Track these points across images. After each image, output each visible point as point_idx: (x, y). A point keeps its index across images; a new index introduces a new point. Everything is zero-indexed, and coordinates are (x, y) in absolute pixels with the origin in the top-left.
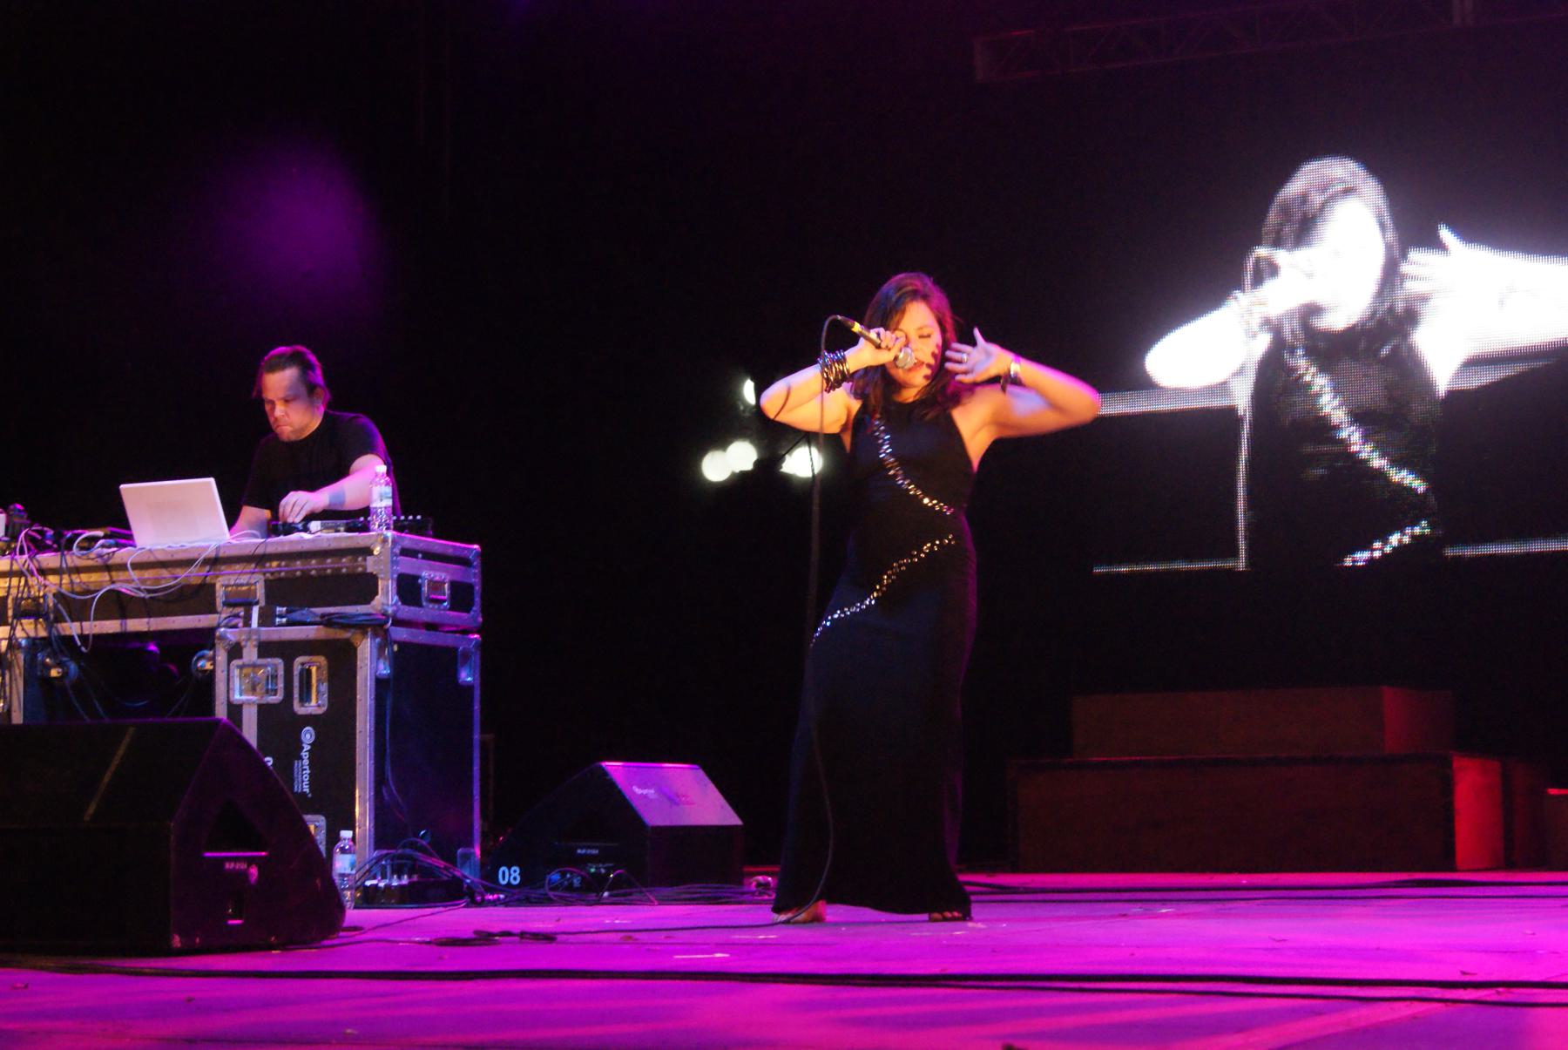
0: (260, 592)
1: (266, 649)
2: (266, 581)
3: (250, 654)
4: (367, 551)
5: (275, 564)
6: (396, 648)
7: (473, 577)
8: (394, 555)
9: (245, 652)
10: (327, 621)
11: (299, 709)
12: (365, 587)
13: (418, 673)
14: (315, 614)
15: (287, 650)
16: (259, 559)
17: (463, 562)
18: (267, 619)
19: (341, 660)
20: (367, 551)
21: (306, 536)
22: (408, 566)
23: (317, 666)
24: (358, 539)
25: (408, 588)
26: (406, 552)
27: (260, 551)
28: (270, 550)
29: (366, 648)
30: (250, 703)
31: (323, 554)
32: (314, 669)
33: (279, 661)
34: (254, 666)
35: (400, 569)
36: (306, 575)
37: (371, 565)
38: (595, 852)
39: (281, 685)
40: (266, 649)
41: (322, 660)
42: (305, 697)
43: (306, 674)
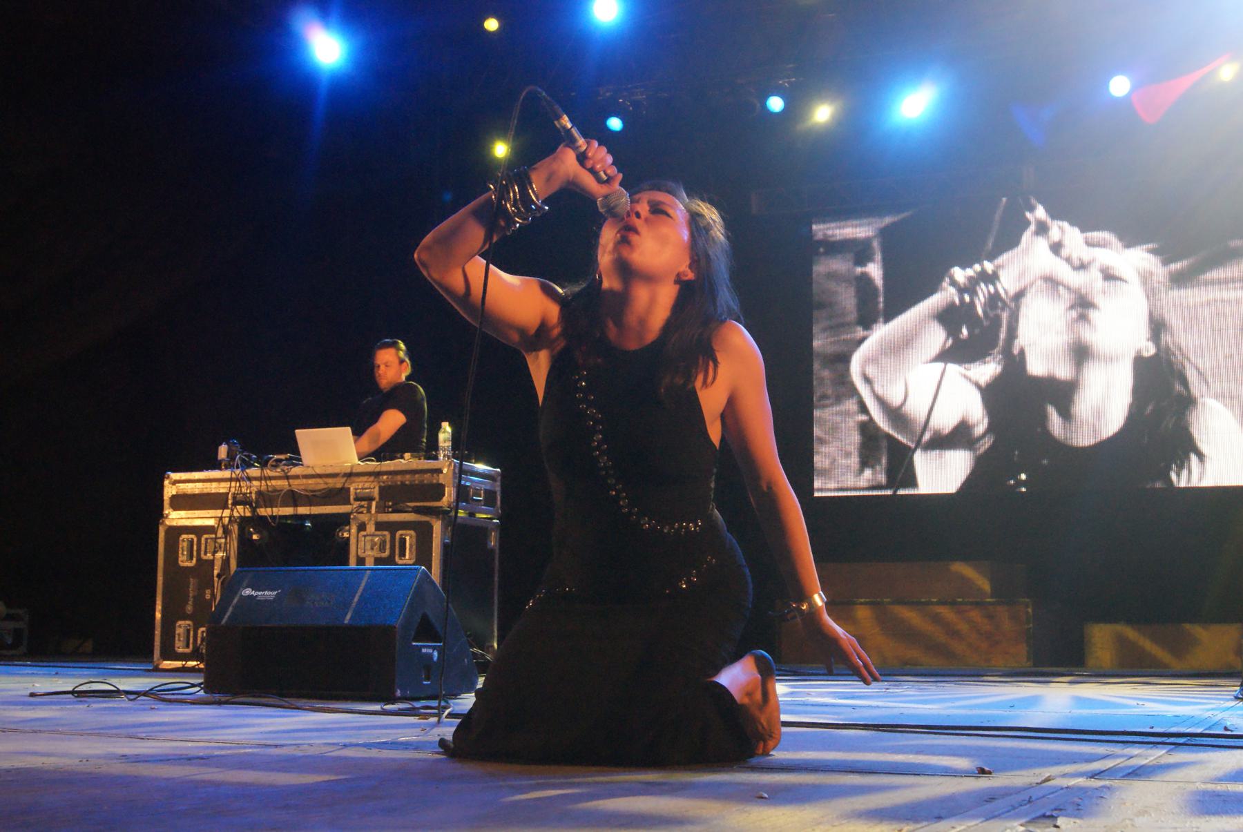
1: (380, 526)
3: (371, 528)
4: (439, 471)
10: (417, 510)
12: (438, 491)
15: (392, 527)
16: (377, 474)
19: (424, 533)
20: (439, 471)
23: (410, 538)
24: (430, 464)
27: (378, 470)
28: (384, 469)
29: (437, 526)
34: (373, 535)
37: (441, 479)
39: (388, 546)
40: (380, 526)
41: (412, 533)
43: (403, 542)
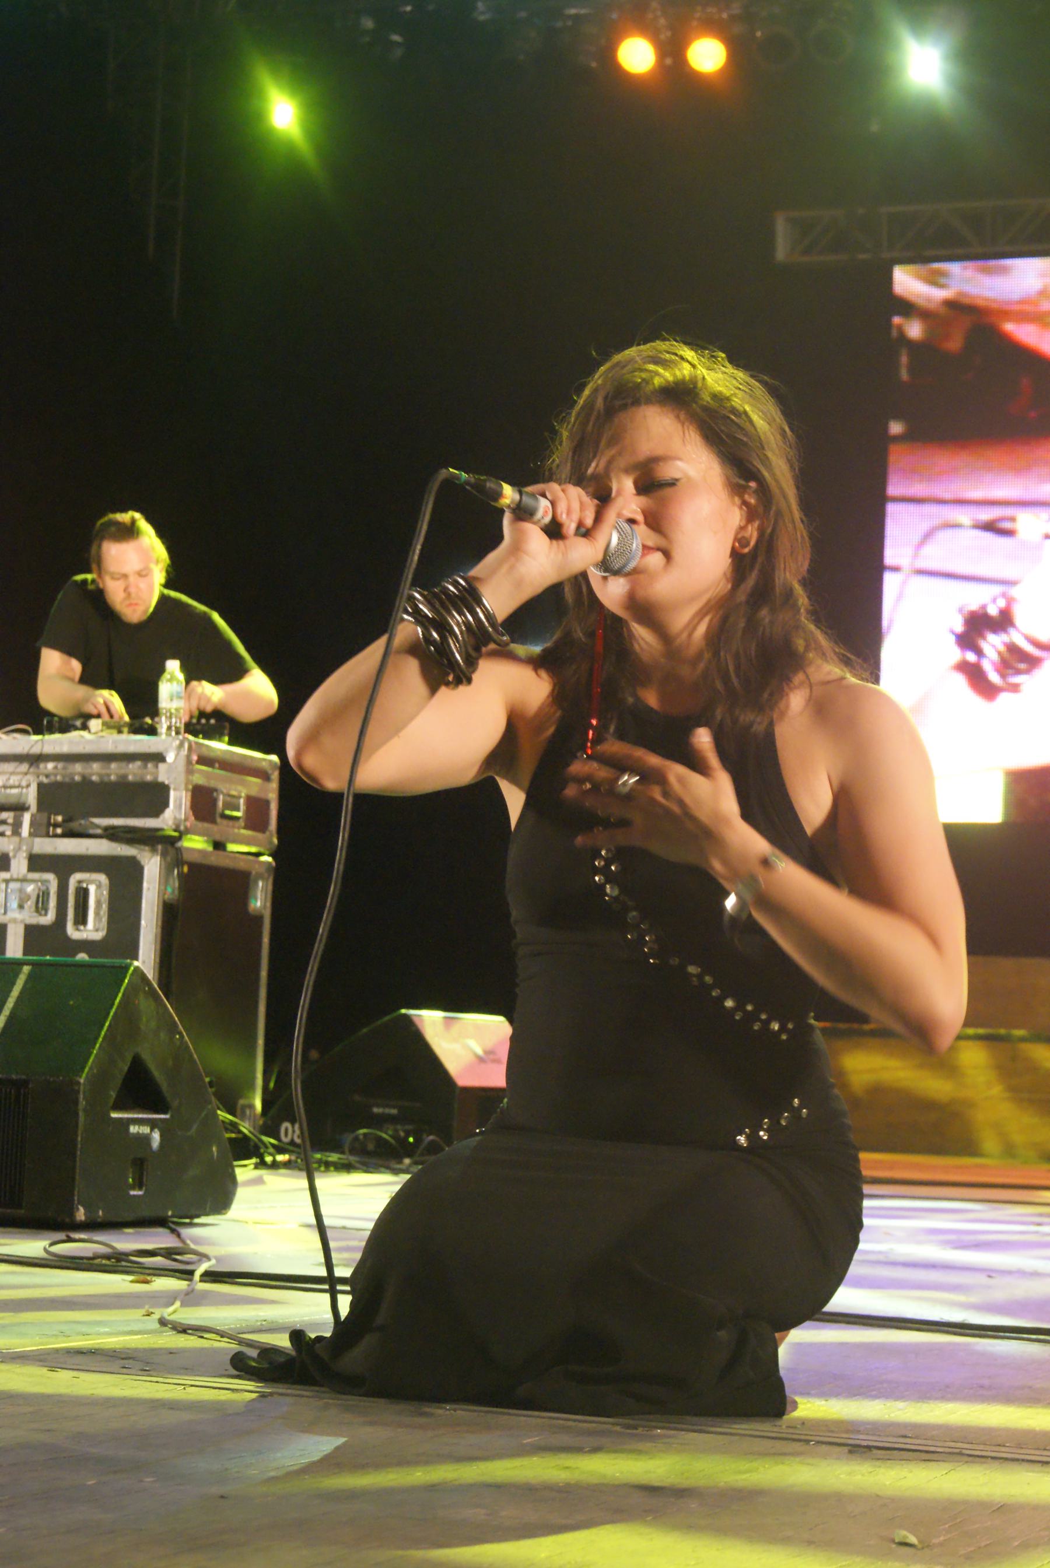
0: (31, 797)
1: (37, 862)
2: (40, 786)
3: (19, 865)
4: (159, 758)
5: (50, 766)
6: (186, 869)
7: (272, 793)
8: (189, 762)
9: (14, 864)
10: (112, 834)
11: (73, 933)
12: (154, 797)
13: (205, 896)
14: (98, 826)
15: (62, 866)
16: (35, 760)
17: (265, 776)
18: (41, 829)
19: (125, 878)
20: (159, 758)
21: (84, 733)
22: (202, 776)
23: (97, 887)
24: (140, 743)
25: (203, 803)
26: (204, 760)
27: (36, 750)
28: (48, 749)
29: (152, 866)
30: (15, 921)
31: (108, 758)
32: (92, 888)
33: (51, 878)
34: (24, 880)
35: (198, 779)
36: (86, 781)
37: (162, 774)
38: (394, 1111)
39: (53, 903)
40: (37, 862)
41: (103, 878)
42: (81, 919)
43: (82, 894)
